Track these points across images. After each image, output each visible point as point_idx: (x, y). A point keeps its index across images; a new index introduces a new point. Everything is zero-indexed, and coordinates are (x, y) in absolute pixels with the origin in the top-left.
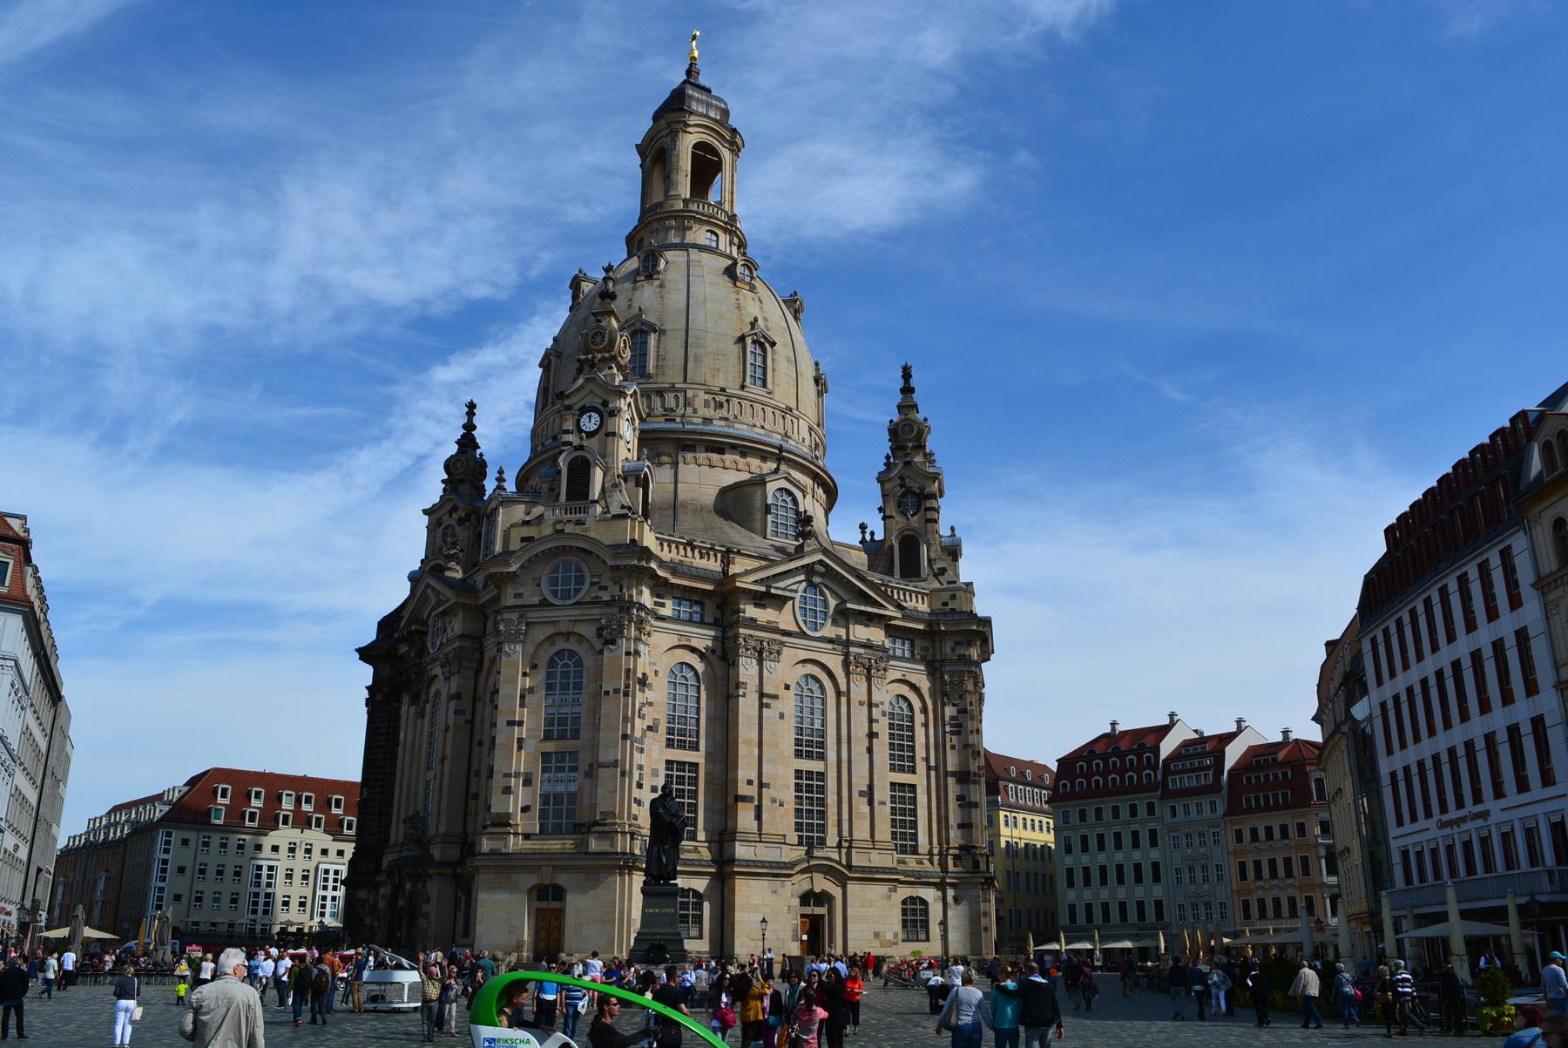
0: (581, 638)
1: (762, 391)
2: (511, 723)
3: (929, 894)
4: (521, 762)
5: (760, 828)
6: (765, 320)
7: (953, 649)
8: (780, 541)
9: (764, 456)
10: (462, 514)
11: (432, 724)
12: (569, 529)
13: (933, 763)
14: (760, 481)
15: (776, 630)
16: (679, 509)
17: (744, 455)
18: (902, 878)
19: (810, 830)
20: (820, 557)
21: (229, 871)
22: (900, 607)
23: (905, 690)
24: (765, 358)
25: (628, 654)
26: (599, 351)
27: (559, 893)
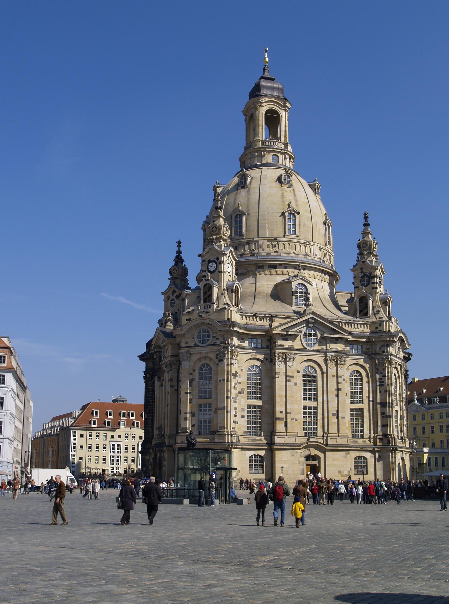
0: (211, 359)
1: (294, 236)
3: (368, 455)
4: (189, 408)
5: (286, 431)
6: (296, 201)
7: (380, 348)
8: (297, 309)
9: (295, 267)
10: (178, 294)
11: (165, 390)
12: (204, 315)
13: (371, 399)
14: (288, 282)
16: (257, 296)
17: (285, 267)
18: (351, 449)
19: (310, 430)
20: (311, 316)
21: (101, 447)
22: (350, 333)
23: (358, 368)
24: (295, 220)
26: (214, 235)
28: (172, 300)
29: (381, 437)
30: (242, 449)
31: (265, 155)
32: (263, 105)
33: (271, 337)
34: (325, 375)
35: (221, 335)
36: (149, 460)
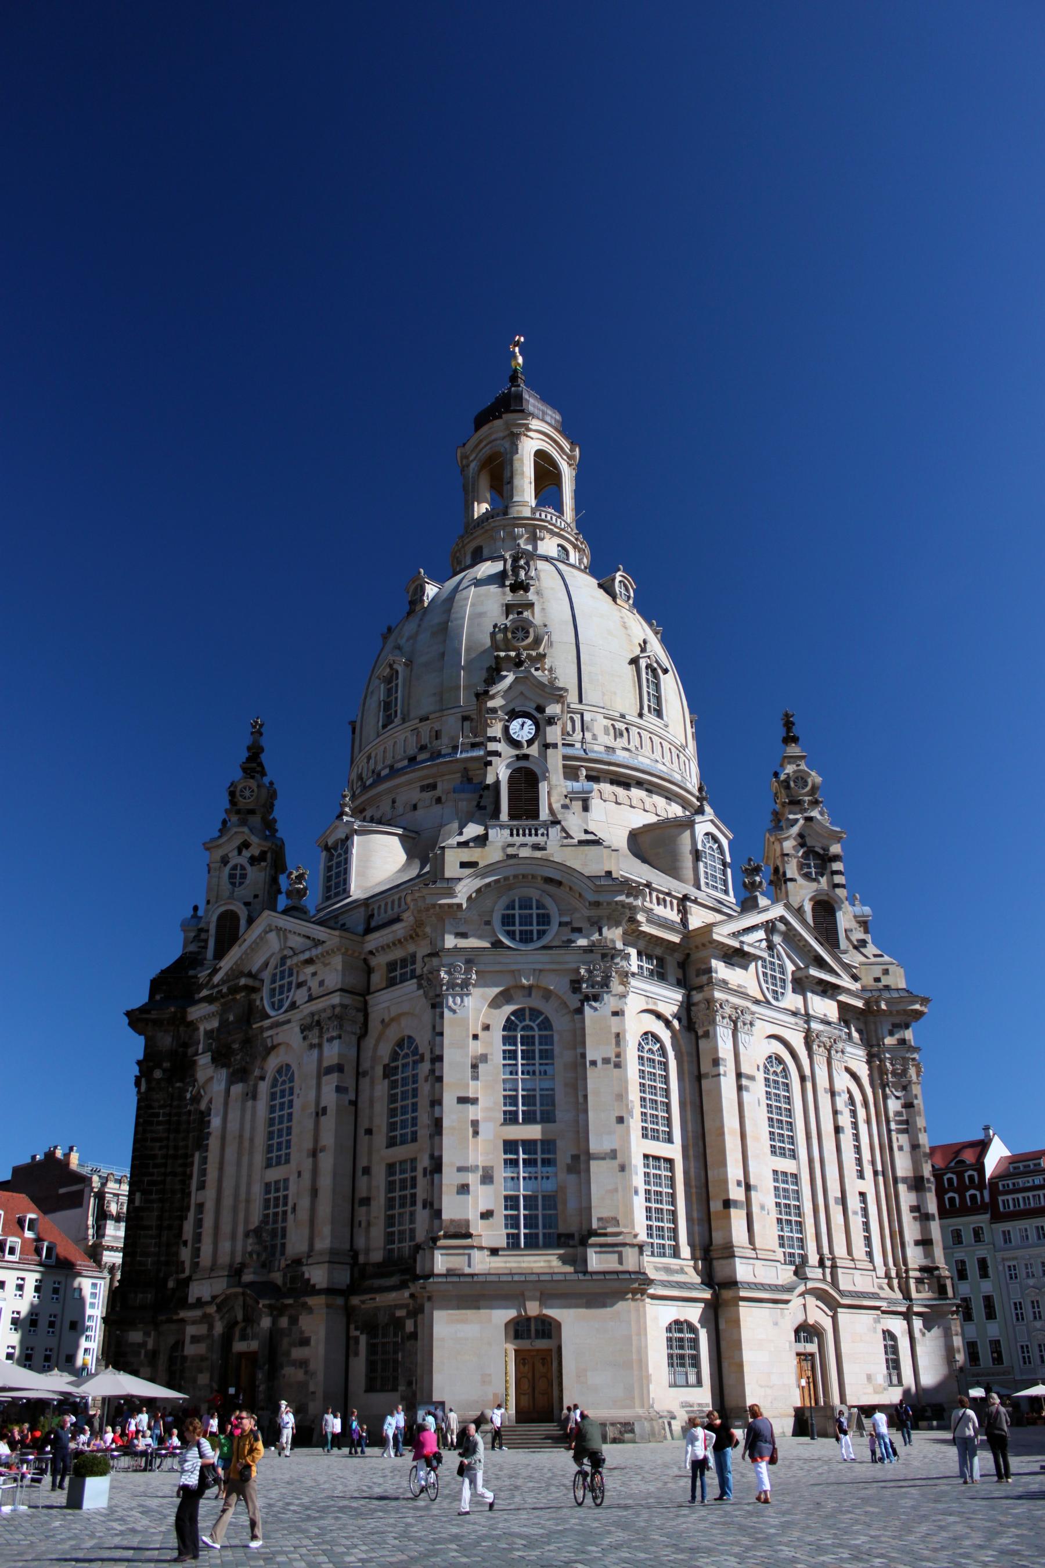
2: (463, 1100)
3: (898, 1326)
5: (751, 1241)
9: (670, 796)
10: (257, 853)
12: (525, 853)
13: (879, 1168)
15: (745, 996)
18: (884, 1305)
25: (615, 1014)
27: (548, 1329)
28: (235, 868)
29: (917, 1274)
30: (653, 1297)
31: (542, 539)
32: (530, 434)
33: (688, 955)
34: (809, 1085)
35: (589, 919)
36: (144, 1344)
